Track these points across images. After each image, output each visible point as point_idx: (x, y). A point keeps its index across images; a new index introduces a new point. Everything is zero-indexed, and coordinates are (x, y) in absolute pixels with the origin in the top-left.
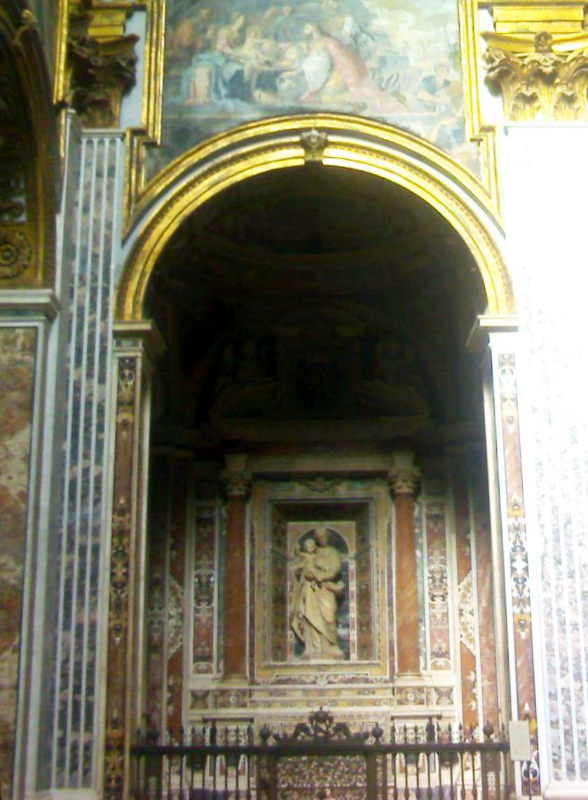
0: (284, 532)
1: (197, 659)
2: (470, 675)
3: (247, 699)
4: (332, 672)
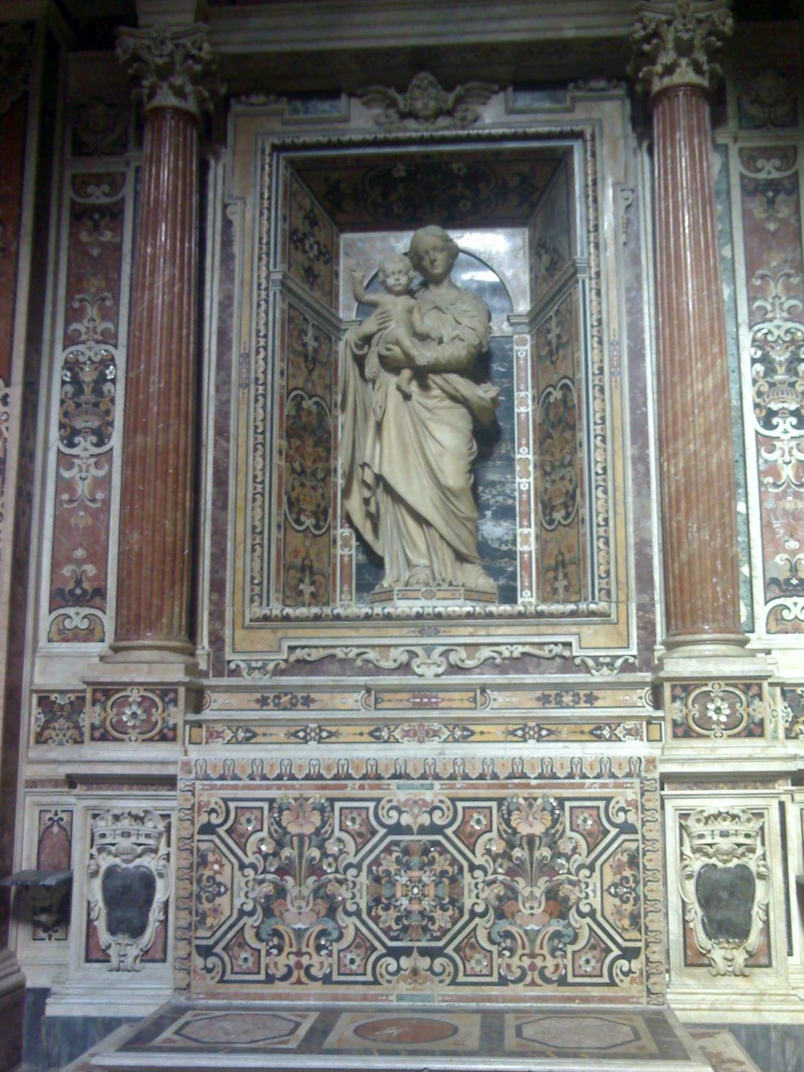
0: (329, 255)
1: (60, 598)
3: (178, 715)
4: (463, 635)
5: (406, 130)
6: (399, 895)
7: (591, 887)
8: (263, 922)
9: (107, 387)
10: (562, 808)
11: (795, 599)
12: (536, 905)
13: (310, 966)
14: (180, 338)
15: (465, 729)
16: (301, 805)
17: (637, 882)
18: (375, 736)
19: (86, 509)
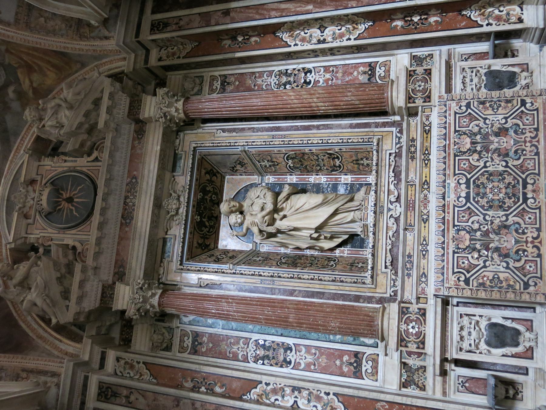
0: (226, 252)
1: (357, 374)
2: (397, 26)
3: (414, 308)
4: (384, 197)
5: (183, 213)
6: (498, 198)
7: (494, 119)
8: (512, 258)
9: (267, 344)
10: (459, 131)
11: (377, 72)
12: (502, 141)
13: (533, 237)
14: (250, 300)
15: (424, 184)
16: (456, 239)
17: (492, 101)
18: (425, 221)
19: (318, 358)
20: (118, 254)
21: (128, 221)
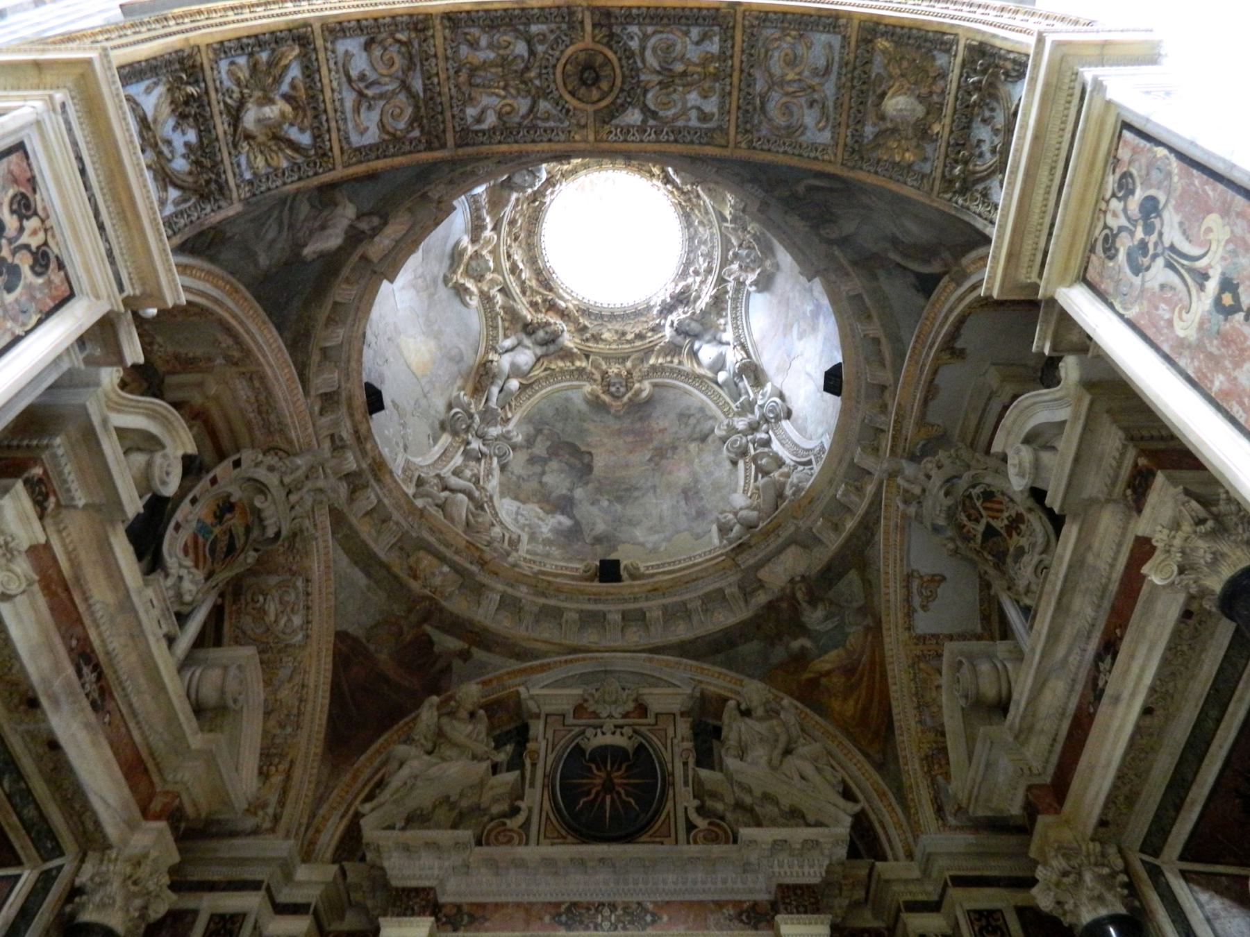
20: (498, 906)
21: (564, 918)
